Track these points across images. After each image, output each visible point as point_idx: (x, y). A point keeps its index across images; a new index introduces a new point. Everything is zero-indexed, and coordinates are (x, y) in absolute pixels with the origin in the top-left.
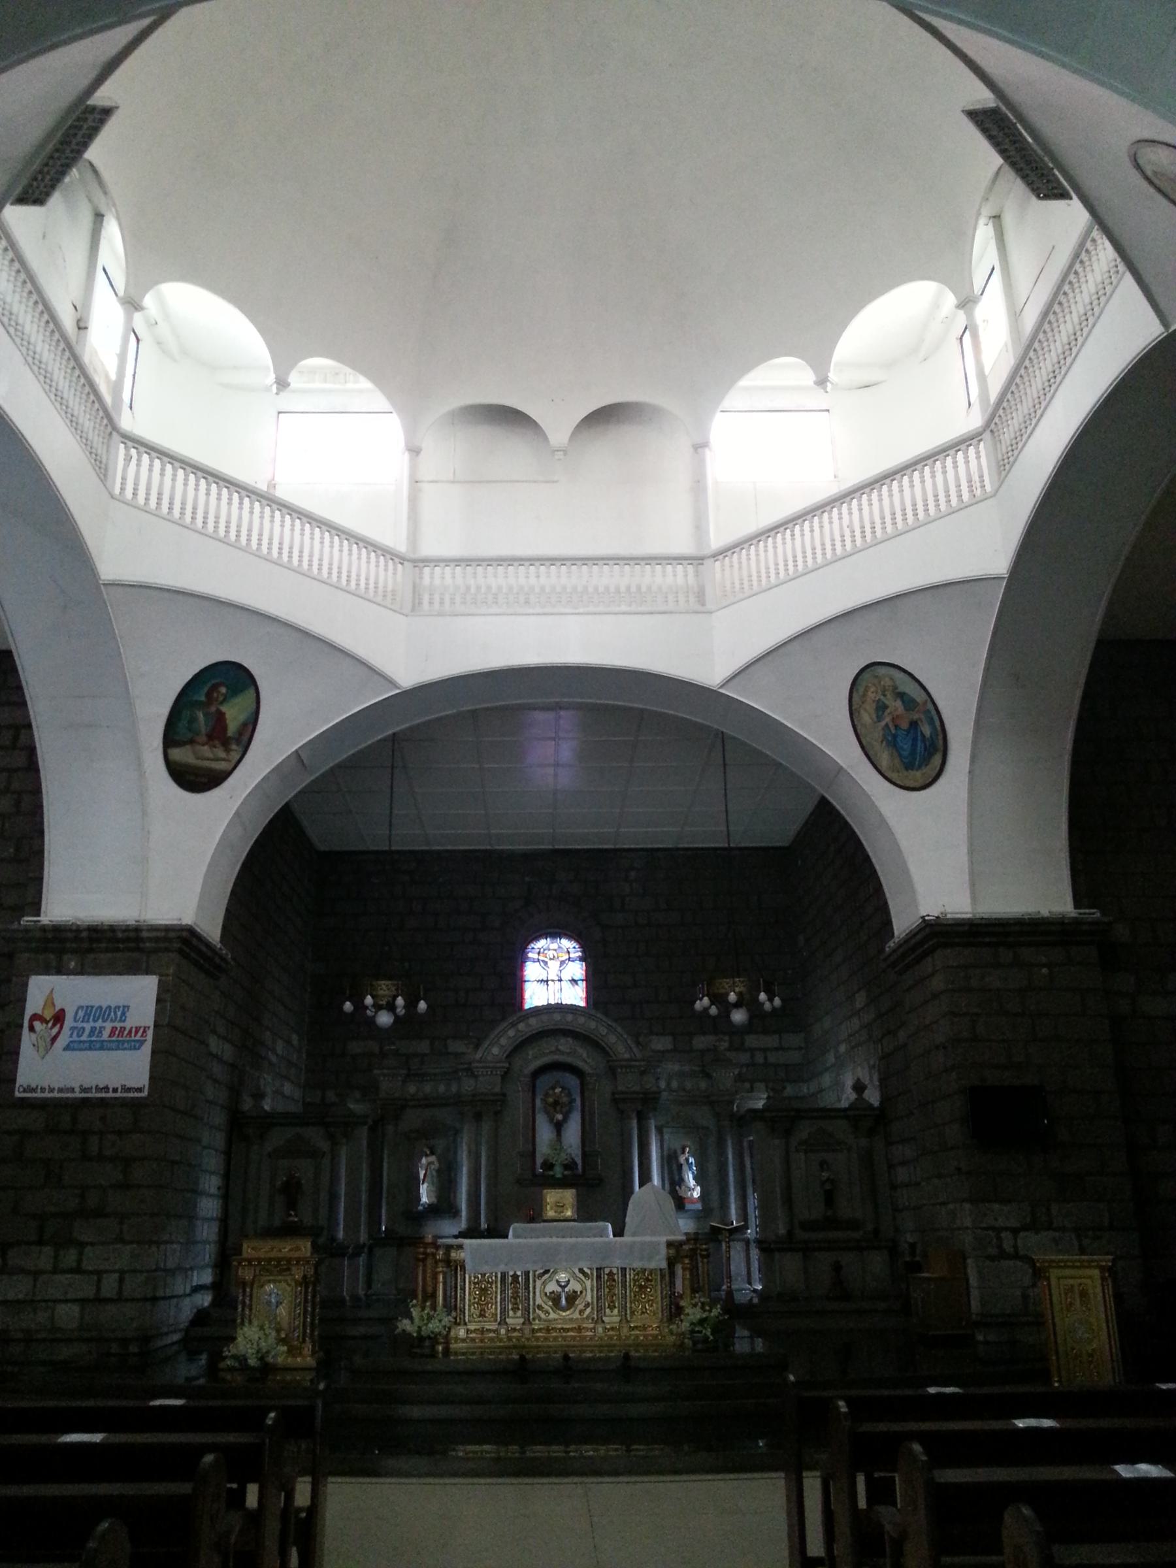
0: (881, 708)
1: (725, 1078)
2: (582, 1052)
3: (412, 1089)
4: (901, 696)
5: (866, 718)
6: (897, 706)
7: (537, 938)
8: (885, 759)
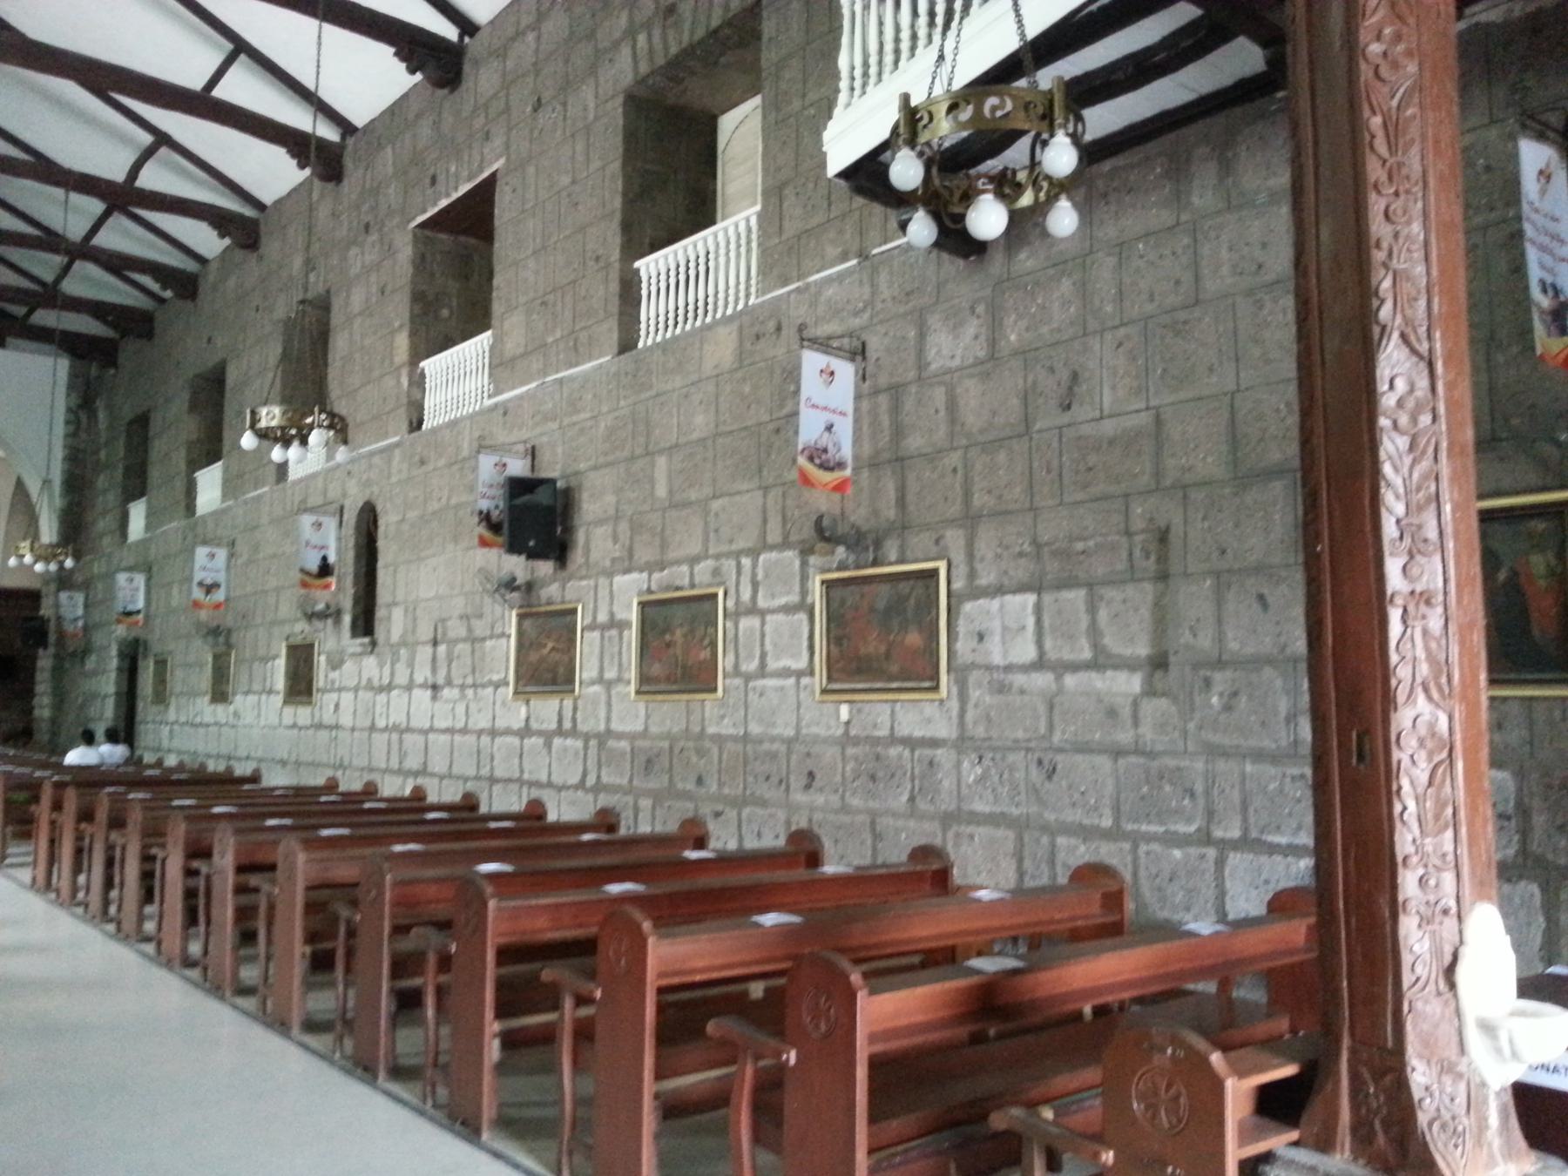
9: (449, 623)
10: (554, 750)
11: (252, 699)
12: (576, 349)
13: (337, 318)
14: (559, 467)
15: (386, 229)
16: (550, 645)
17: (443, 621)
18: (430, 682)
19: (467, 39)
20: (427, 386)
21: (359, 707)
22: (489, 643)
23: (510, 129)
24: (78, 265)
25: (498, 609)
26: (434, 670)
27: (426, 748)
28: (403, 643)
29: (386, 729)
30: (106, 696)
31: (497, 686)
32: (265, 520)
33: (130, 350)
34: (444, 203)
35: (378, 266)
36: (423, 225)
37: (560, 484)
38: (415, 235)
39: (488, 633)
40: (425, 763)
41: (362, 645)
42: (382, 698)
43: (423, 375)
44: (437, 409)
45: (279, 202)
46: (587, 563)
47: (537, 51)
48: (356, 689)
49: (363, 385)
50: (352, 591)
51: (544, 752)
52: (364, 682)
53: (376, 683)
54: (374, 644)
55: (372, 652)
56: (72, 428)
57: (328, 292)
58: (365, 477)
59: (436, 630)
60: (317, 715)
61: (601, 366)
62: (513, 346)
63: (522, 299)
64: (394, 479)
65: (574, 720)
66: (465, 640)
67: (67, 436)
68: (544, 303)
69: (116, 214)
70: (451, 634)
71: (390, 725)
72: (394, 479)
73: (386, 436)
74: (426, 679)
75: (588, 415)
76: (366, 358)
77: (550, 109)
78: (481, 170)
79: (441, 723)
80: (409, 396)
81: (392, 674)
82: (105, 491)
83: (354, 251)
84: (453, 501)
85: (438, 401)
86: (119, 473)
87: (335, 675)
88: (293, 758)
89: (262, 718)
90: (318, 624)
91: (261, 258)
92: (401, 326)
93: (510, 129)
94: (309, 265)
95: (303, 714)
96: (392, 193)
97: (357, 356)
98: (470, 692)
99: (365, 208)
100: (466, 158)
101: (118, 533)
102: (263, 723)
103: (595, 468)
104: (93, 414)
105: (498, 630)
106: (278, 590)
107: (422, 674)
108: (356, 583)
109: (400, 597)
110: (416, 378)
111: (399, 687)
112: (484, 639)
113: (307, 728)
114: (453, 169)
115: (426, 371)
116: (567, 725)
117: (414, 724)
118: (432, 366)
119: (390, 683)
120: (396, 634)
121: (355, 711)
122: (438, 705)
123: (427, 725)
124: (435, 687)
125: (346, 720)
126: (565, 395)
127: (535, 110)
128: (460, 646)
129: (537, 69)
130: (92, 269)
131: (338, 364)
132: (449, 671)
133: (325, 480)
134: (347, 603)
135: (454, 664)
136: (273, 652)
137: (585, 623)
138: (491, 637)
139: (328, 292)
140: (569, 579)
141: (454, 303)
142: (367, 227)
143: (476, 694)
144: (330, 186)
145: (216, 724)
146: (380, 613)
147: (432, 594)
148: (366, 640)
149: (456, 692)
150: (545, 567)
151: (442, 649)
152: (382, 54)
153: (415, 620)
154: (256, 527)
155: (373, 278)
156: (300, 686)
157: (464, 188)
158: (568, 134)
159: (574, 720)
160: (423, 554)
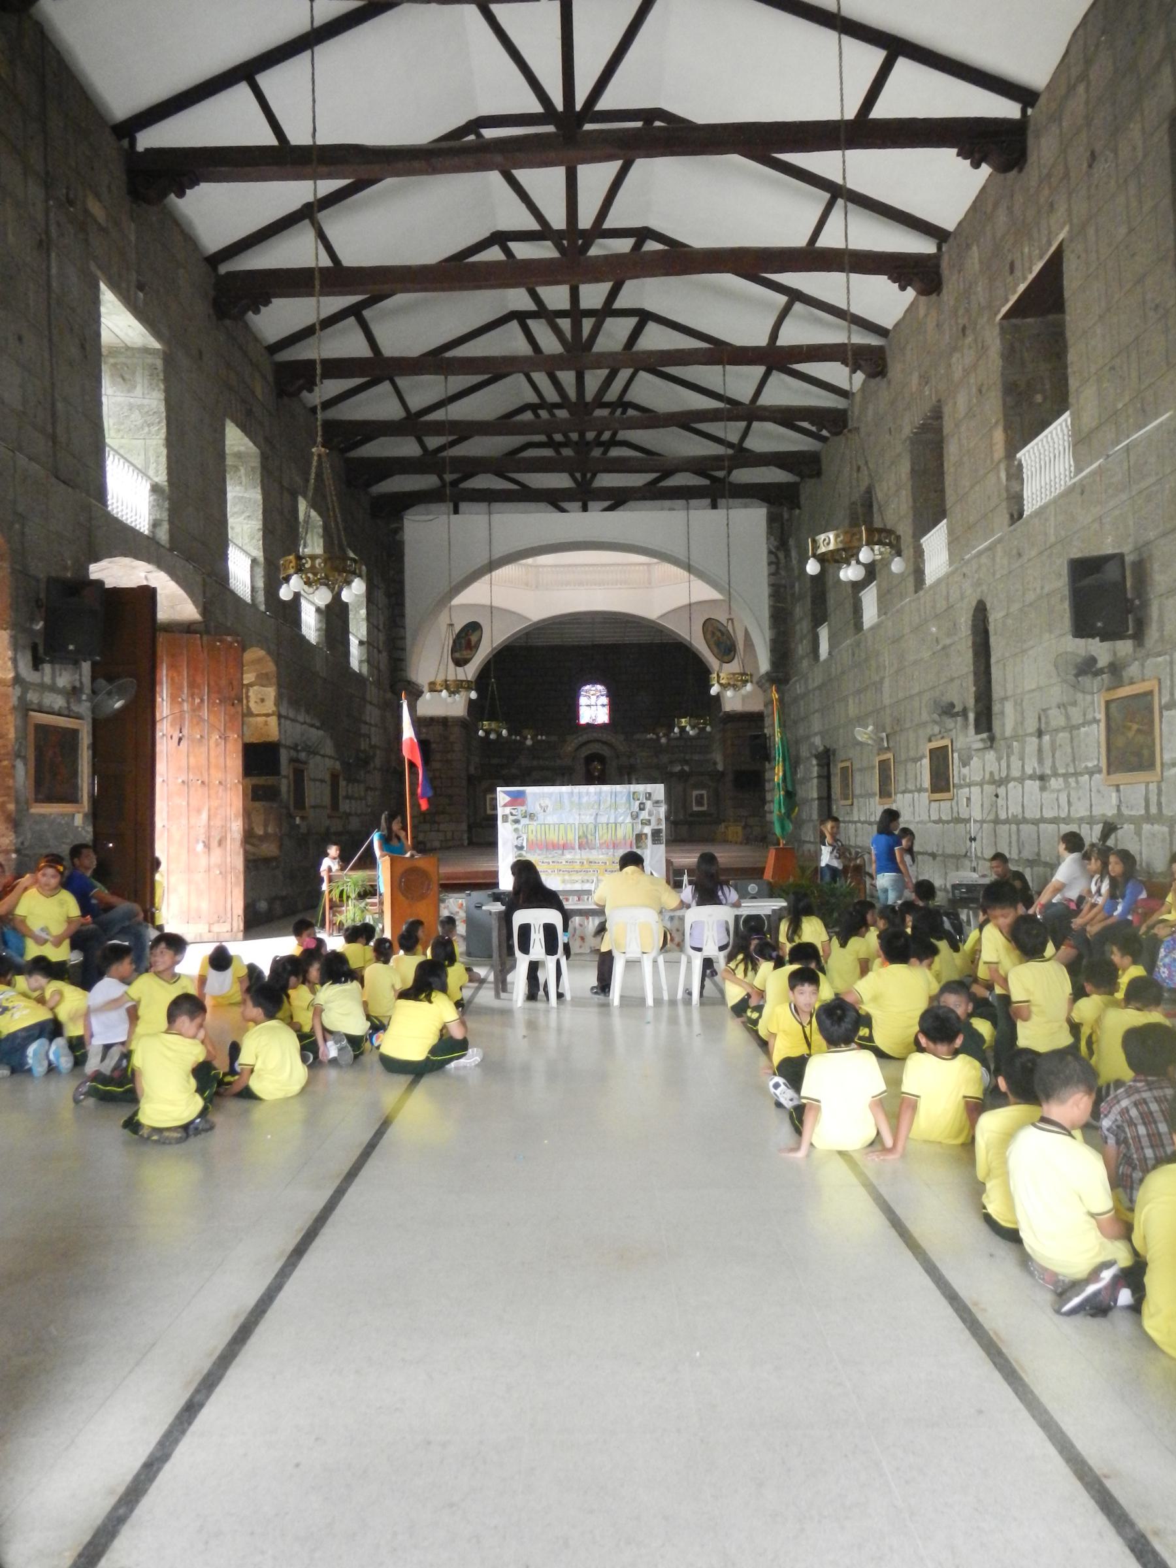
0: (713, 634)
1: (665, 759)
2: (605, 748)
3: (535, 763)
4: (720, 631)
5: (709, 636)
6: (719, 634)
7: (585, 685)
8: (716, 650)
9: (1050, 712)
10: (1143, 838)
11: (908, 796)
12: (1144, 411)
13: (948, 426)
14: (1130, 540)
15: (978, 327)
16: (1135, 727)
17: (1044, 710)
18: (1038, 772)
19: (1030, 111)
20: (1025, 476)
21: (985, 799)
22: (1083, 730)
23: (1070, 194)
24: (755, 424)
25: (1089, 697)
26: (1041, 760)
27: (1039, 836)
28: (1015, 737)
29: (1007, 821)
30: (813, 800)
31: (1091, 773)
32: (907, 630)
33: (808, 488)
34: (1022, 287)
35: (975, 366)
36: (1007, 316)
37: (1129, 559)
38: (1002, 328)
39: (1081, 721)
40: (1038, 854)
41: (982, 740)
42: (1001, 791)
43: (1020, 466)
44: (1034, 496)
45: (897, 325)
46: (1162, 638)
47: (1087, 103)
48: (981, 784)
49: (972, 487)
50: (973, 689)
51: (1136, 838)
52: (987, 776)
53: (997, 778)
54: (992, 739)
55: (991, 747)
56: (774, 567)
57: (939, 401)
58: (976, 576)
59: (1040, 719)
60: (955, 809)
61: (1161, 424)
62: (1089, 419)
63: (1093, 370)
64: (998, 576)
65: (1159, 804)
66: (1064, 729)
67: (770, 575)
68: (1113, 368)
69: (775, 373)
70: (1054, 724)
71: (1010, 815)
72: (998, 576)
73: (993, 533)
74: (1034, 768)
75: (1152, 480)
76: (972, 460)
77: (1103, 159)
78: (1050, 244)
79: (1048, 814)
80: (1007, 490)
81: (1008, 766)
82: (801, 619)
83: (957, 355)
84: (1046, 590)
85: (1034, 491)
86: (809, 600)
87: (965, 771)
88: (940, 852)
89: (916, 815)
90: (949, 723)
91: (889, 382)
92: (996, 423)
93: (1070, 194)
94: (925, 379)
95: (943, 809)
96: (980, 292)
97: (965, 459)
98: (1072, 780)
99: (961, 312)
100: (1035, 235)
101: (811, 655)
102: (917, 819)
103: (1164, 535)
104: (788, 555)
105: (1089, 717)
106: (920, 693)
107: (1031, 766)
108: (976, 683)
109: (1009, 693)
110: (1013, 470)
111: (1014, 779)
112: (1078, 727)
113: (948, 822)
114: (1026, 250)
115: (1023, 462)
116: (1154, 810)
117: (1028, 815)
118: (1026, 455)
119: (1008, 775)
120: (1008, 733)
121: (982, 805)
122: (1045, 795)
123: (1038, 816)
124: (1042, 778)
126: (1132, 462)
127: (1090, 166)
128: (1061, 735)
129: (1088, 120)
130: (770, 426)
131: (952, 470)
132: (1054, 762)
133: (947, 584)
134: (971, 702)
135: (1057, 754)
136: (920, 754)
137: (1163, 702)
138: (1083, 725)
139: (939, 401)
140: (1148, 656)
141: (1047, 387)
142: (964, 329)
143: (1077, 782)
144: (934, 297)
146: (996, 708)
147: (1033, 687)
148: (985, 735)
149: (1061, 780)
150: (1124, 647)
151: (1046, 738)
152: (946, 158)
153: (1022, 713)
154: (903, 636)
155: (972, 381)
156: (941, 782)
157: (1037, 268)
158: (1121, 181)
159: (1159, 804)
160: (1025, 646)
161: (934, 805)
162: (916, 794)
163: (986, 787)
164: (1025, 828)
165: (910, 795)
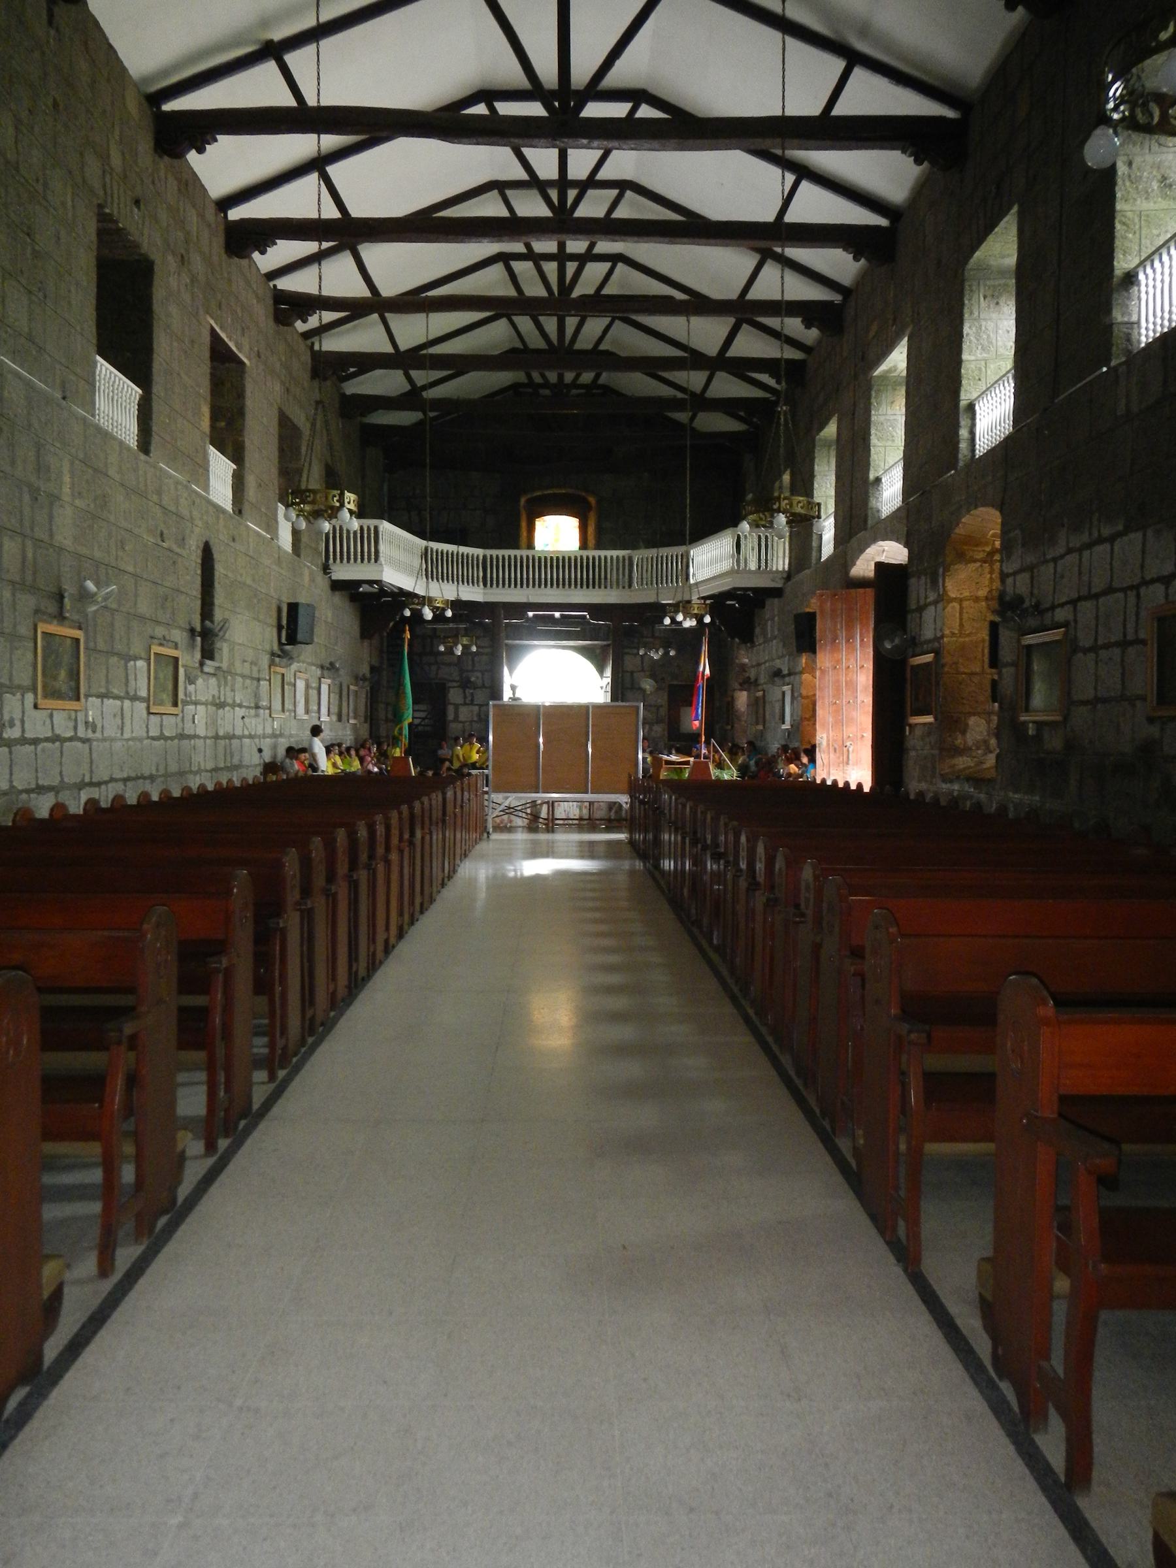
42: (221, 711)
60: (180, 725)
87: (191, 688)
88: (162, 772)
89: (127, 729)
102: (127, 735)
111: (228, 705)
125: (201, 732)
145: (55, 738)
161: (154, 719)
162: (127, 703)
163: (209, 707)
164: (235, 742)
165: (118, 703)
